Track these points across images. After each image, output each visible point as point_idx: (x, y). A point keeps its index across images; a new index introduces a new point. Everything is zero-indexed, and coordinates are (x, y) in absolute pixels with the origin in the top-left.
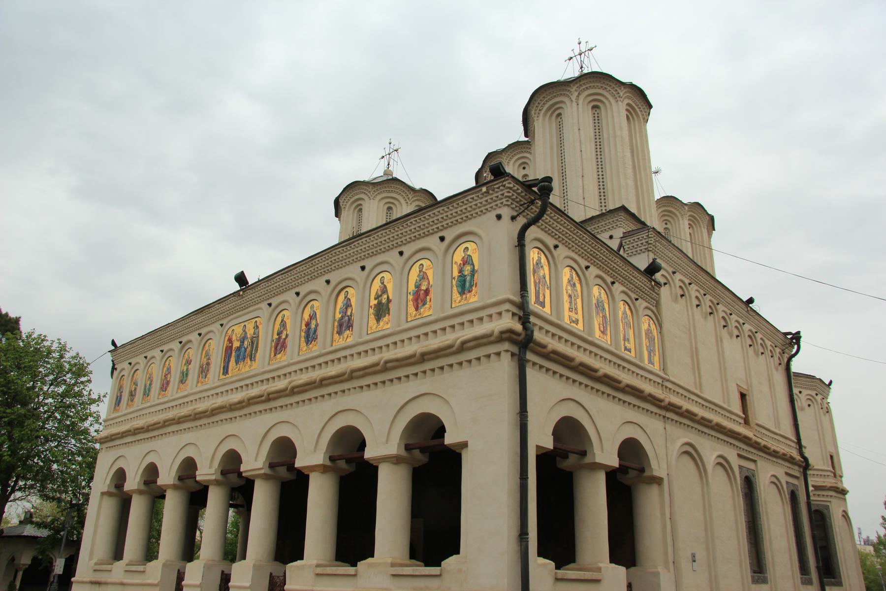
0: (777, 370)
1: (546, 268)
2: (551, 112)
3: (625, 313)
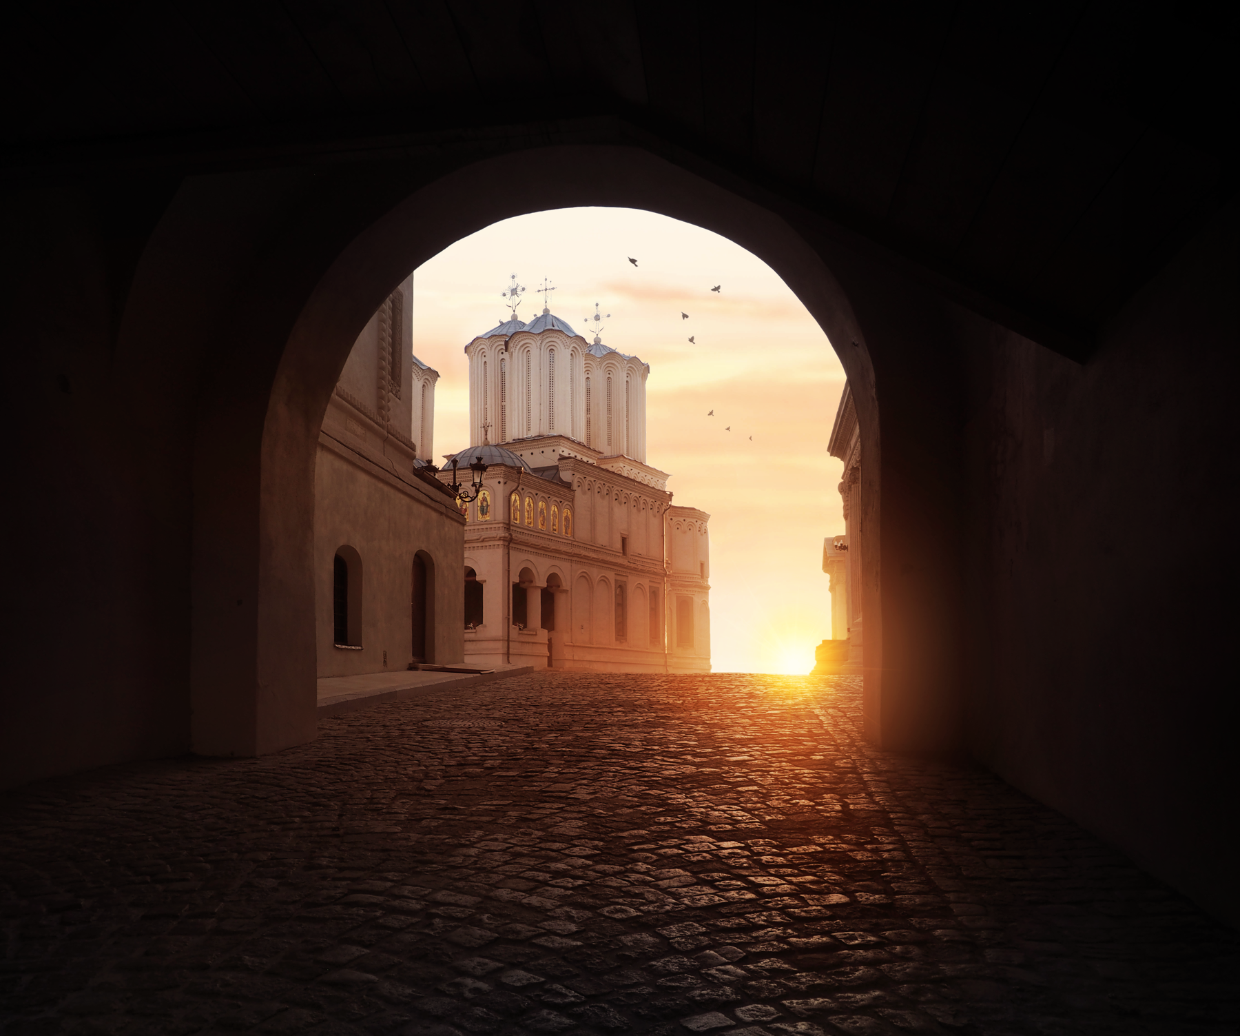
0: (655, 516)
1: (518, 502)
2: (521, 351)
3: (554, 511)
